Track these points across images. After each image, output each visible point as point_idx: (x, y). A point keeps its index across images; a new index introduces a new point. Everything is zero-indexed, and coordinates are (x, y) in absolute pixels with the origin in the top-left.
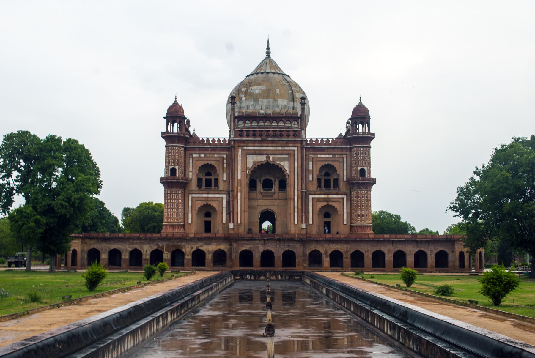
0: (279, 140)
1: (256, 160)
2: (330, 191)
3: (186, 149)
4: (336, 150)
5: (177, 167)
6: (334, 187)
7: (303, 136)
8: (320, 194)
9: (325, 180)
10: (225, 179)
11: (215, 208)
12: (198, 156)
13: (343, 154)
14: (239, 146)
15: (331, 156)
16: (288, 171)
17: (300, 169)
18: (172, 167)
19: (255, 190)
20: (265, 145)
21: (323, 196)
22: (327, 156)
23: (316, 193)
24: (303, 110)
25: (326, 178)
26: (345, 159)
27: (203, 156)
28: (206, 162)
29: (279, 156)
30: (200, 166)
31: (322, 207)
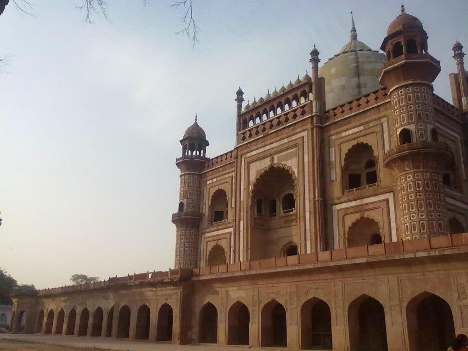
0: (284, 128)
1: (260, 168)
2: (363, 191)
4: (368, 114)
5: (185, 201)
8: (348, 201)
9: (367, 174)
12: (211, 181)
13: (380, 118)
14: (243, 154)
15: (362, 128)
16: (296, 173)
17: (311, 164)
20: (268, 142)
21: (353, 204)
22: (356, 130)
23: (342, 200)
27: (215, 180)
29: (284, 153)
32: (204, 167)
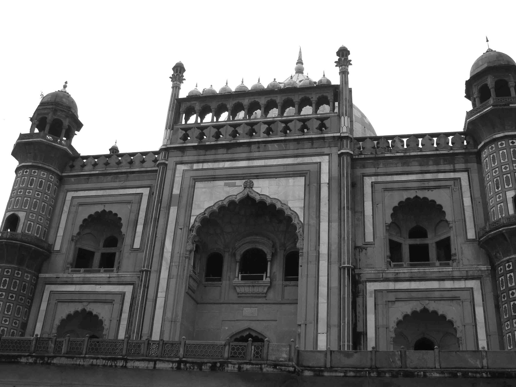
2: (427, 269)
3: (61, 180)
5: (22, 215)
6: (439, 259)
7: (344, 130)
9: (411, 247)
10: (137, 245)
11: (101, 322)
18: (12, 213)
19: (220, 280)
24: (344, 74)
25: (418, 241)
26: (465, 183)
28: (99, 209)
30: (86, 217)
31: (406, 316)
32: (72, 167)
